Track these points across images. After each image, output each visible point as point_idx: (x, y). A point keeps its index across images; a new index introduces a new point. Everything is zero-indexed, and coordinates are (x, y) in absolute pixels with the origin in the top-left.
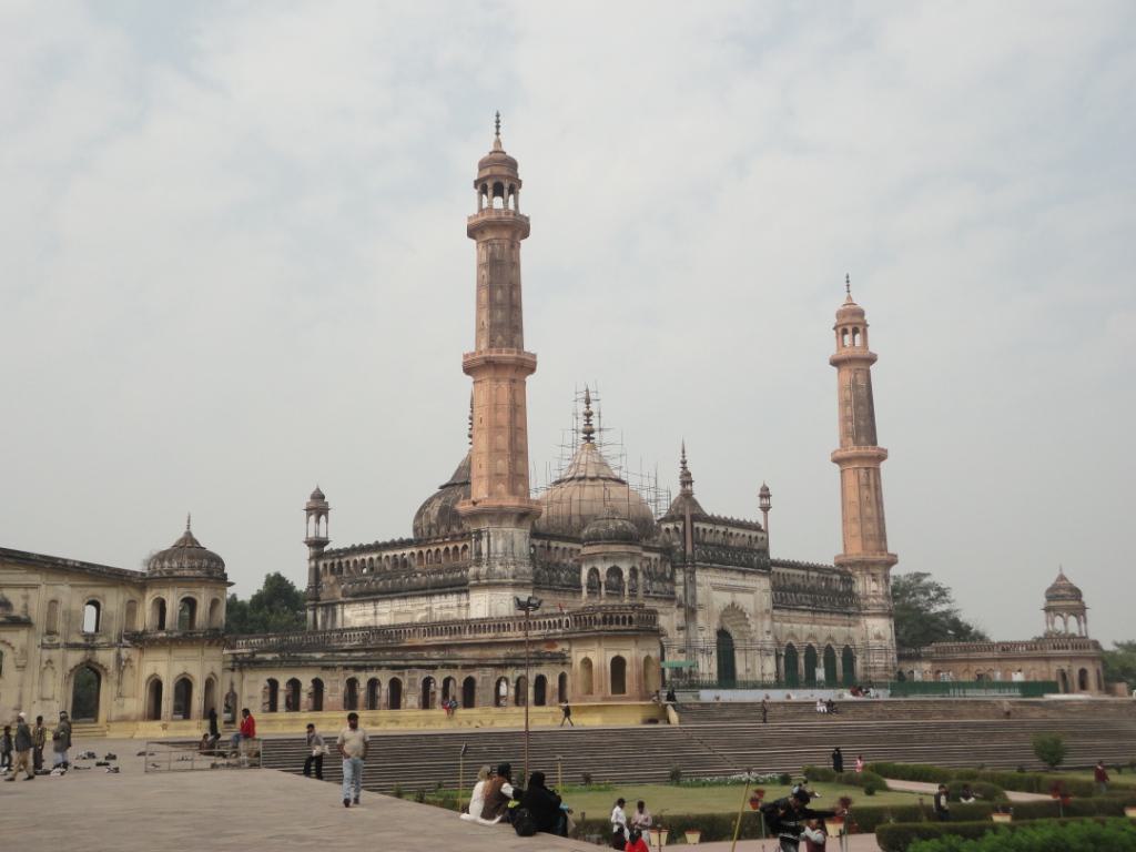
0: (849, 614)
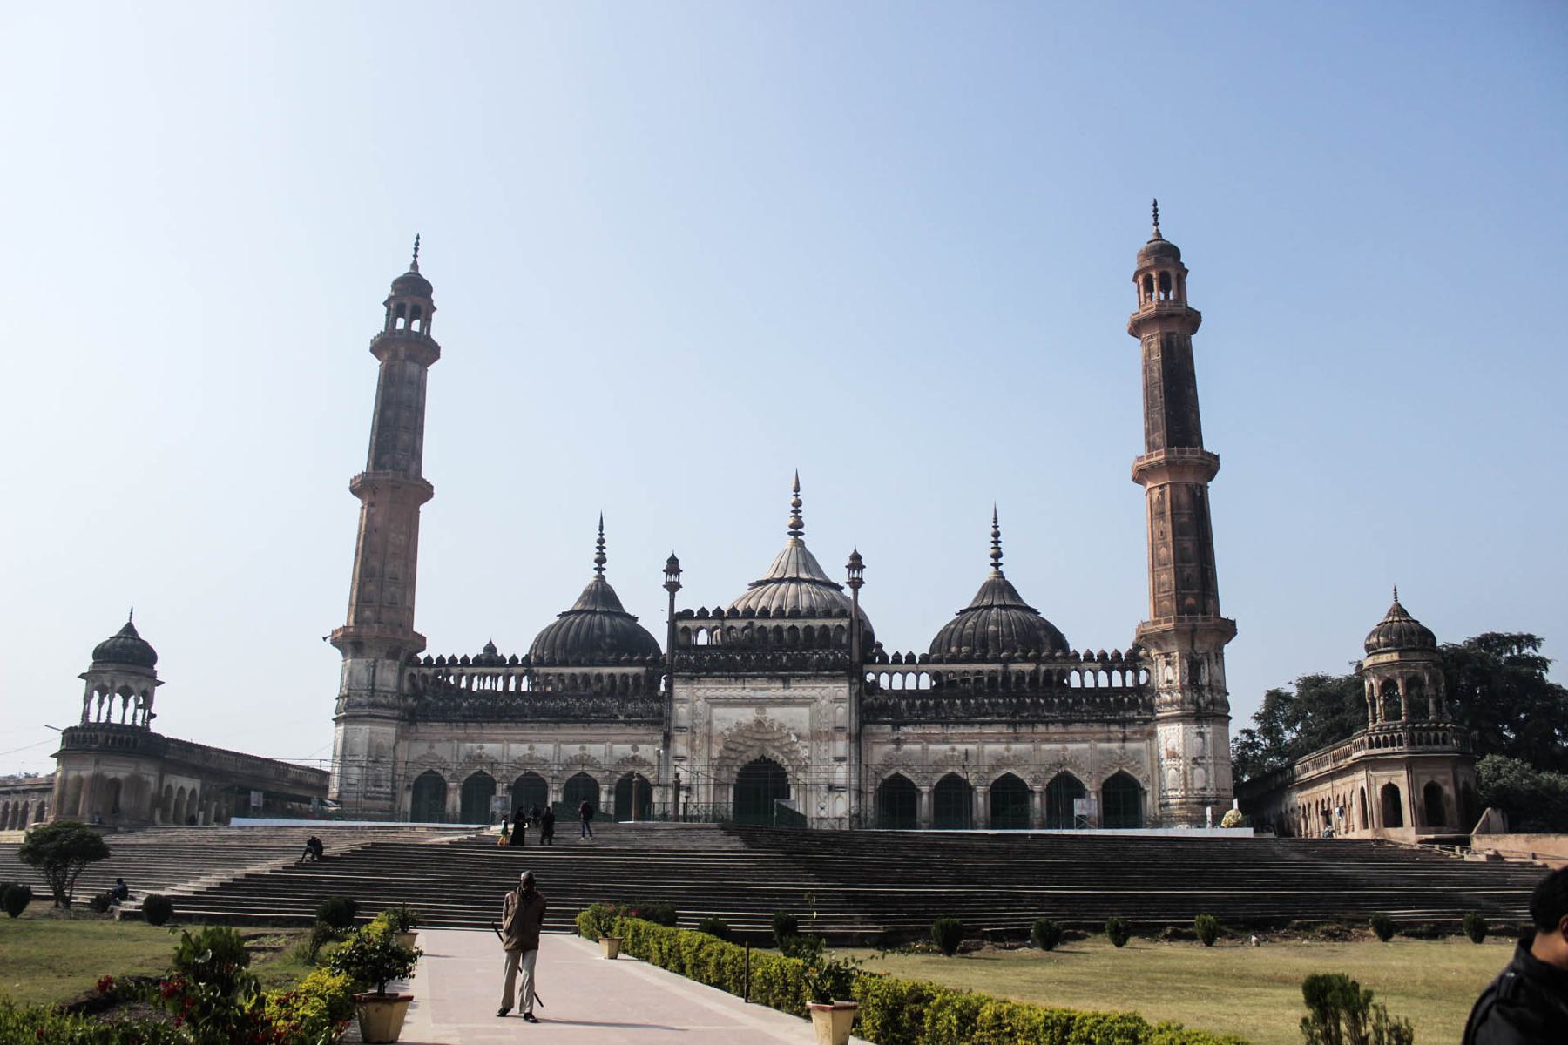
0: (1123, 723)
